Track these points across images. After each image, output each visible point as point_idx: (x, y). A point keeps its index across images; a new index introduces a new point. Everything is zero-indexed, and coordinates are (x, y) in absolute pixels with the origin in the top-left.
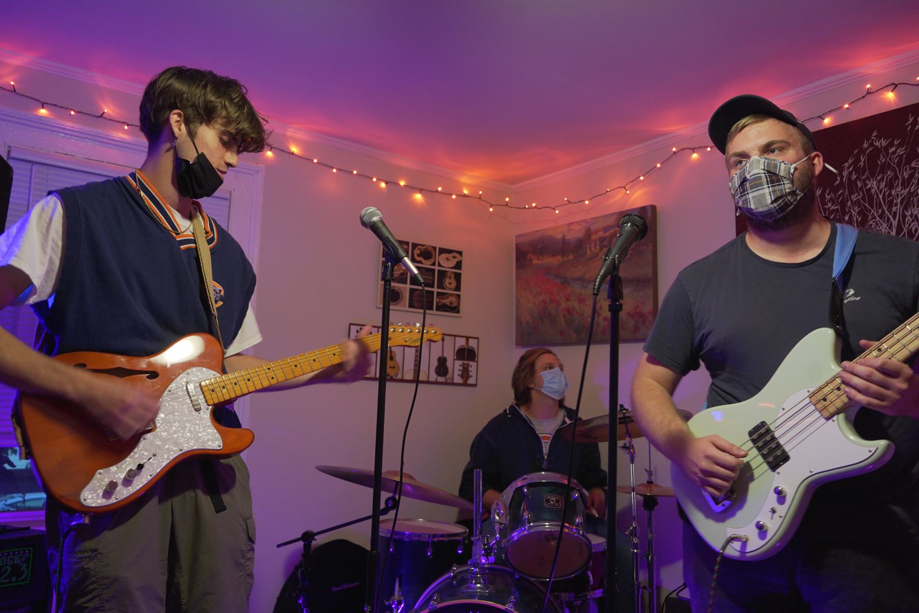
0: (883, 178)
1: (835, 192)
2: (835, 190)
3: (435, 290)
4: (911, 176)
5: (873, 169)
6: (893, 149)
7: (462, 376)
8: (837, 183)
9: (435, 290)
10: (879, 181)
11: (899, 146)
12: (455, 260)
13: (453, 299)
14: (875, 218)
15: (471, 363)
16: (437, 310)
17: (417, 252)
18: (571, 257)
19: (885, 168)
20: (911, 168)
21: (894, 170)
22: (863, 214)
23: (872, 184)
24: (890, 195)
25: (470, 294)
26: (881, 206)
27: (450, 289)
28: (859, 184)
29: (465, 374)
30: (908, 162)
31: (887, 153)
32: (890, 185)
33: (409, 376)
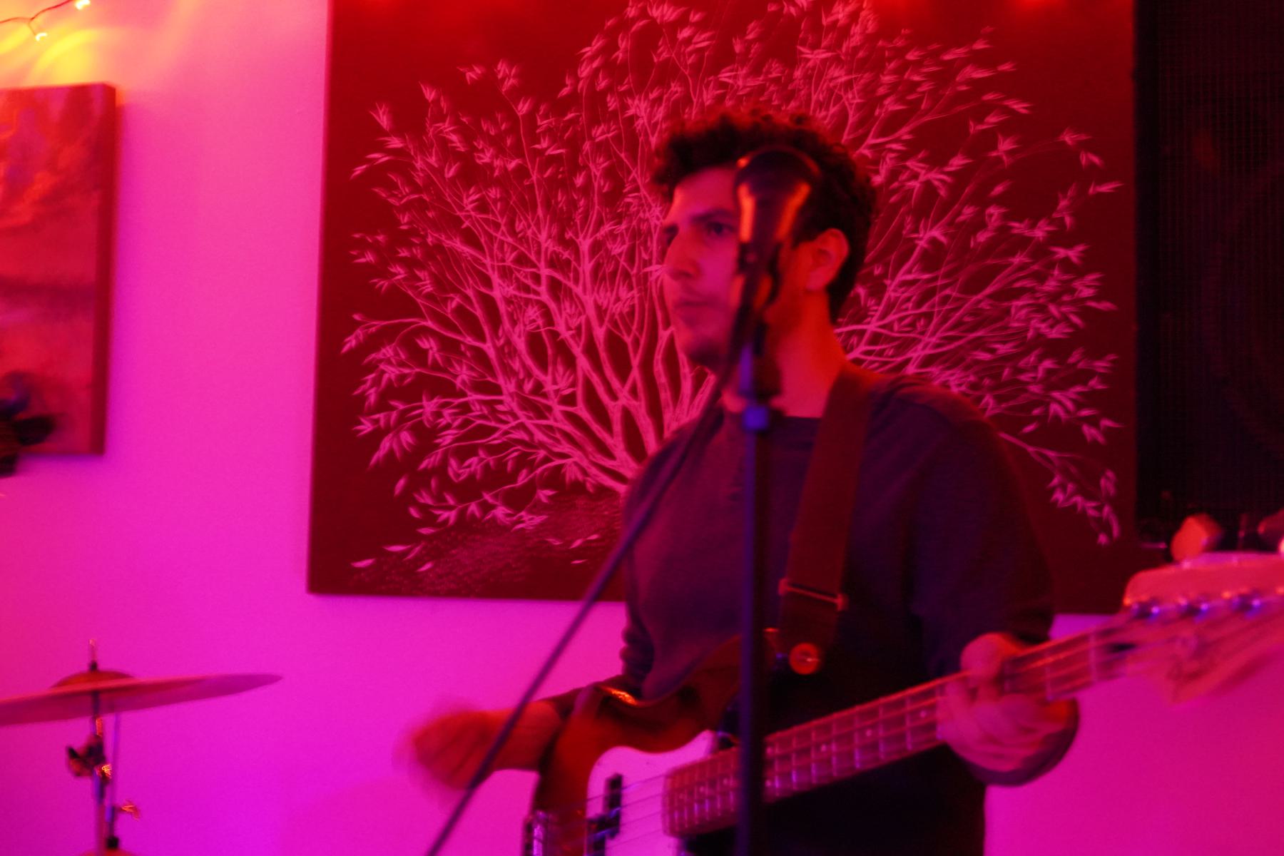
0: (658, 101)
2: (560, 108)
8: (565, 91)
11: (700, 27)
14: (637, 189)
19: (668, 73)
20: (723, 85)
22: (615, 174)
23: (638, 107)
28: (612, 103)
30: (716, 71)
31: (673, 39)
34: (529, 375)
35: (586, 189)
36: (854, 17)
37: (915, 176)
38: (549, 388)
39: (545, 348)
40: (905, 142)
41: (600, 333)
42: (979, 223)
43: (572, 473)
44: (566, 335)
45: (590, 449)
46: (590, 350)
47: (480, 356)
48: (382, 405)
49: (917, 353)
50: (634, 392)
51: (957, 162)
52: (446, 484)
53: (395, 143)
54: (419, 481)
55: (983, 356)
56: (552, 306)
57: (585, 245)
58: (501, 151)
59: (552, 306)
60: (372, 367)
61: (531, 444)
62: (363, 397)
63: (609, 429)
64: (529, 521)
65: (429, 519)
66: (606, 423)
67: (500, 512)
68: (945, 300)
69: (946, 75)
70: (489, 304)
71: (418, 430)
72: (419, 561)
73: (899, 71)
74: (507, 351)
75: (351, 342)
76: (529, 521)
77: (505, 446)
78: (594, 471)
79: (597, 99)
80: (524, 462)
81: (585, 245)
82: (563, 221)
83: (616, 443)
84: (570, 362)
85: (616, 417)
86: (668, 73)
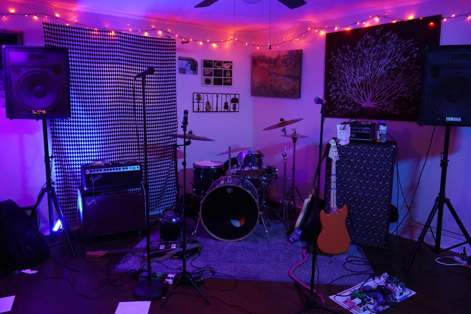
2: (355, 51)
3: (223, 77)
4: (376, 49)
5: (366, 46)
7: (233, 109)
9: (223, 77)
11: (373, 39)
13: (229, 80)
18: (272, 65)
19: (369, 46)
23: (365, 51)
29: (234, 108)
32: (370, 52)
33: (215, 110)
36: (394, 37)
39: (353, 85)
41: (360, 83)
43: (356, 102)
46: (358, 85)
47: (345, 86)
48: (333, 93)
49: (401, 85)
51: (408, 57)
52: (340, 103)
53: (334, 57)
54: (337, 103)
57: (358, 71)
58: (347, 58)
60: (331, 87)
61: (351, 98)
63: (360, 96)
64: (351, 108)
65: (338, 108)
69: (407, 45)
70: (346, 79)
71: (337, 96)
72: (337, 113)
73: (401, 44)
74: (348, 85)
75: (329, 84)
76: (351, 108)
79: (360, 50)
80: (350, 100)
81: (358, 71)
82: (355, 67)
83: (361, 98)
84: (356, 87)
85: (362, 94)
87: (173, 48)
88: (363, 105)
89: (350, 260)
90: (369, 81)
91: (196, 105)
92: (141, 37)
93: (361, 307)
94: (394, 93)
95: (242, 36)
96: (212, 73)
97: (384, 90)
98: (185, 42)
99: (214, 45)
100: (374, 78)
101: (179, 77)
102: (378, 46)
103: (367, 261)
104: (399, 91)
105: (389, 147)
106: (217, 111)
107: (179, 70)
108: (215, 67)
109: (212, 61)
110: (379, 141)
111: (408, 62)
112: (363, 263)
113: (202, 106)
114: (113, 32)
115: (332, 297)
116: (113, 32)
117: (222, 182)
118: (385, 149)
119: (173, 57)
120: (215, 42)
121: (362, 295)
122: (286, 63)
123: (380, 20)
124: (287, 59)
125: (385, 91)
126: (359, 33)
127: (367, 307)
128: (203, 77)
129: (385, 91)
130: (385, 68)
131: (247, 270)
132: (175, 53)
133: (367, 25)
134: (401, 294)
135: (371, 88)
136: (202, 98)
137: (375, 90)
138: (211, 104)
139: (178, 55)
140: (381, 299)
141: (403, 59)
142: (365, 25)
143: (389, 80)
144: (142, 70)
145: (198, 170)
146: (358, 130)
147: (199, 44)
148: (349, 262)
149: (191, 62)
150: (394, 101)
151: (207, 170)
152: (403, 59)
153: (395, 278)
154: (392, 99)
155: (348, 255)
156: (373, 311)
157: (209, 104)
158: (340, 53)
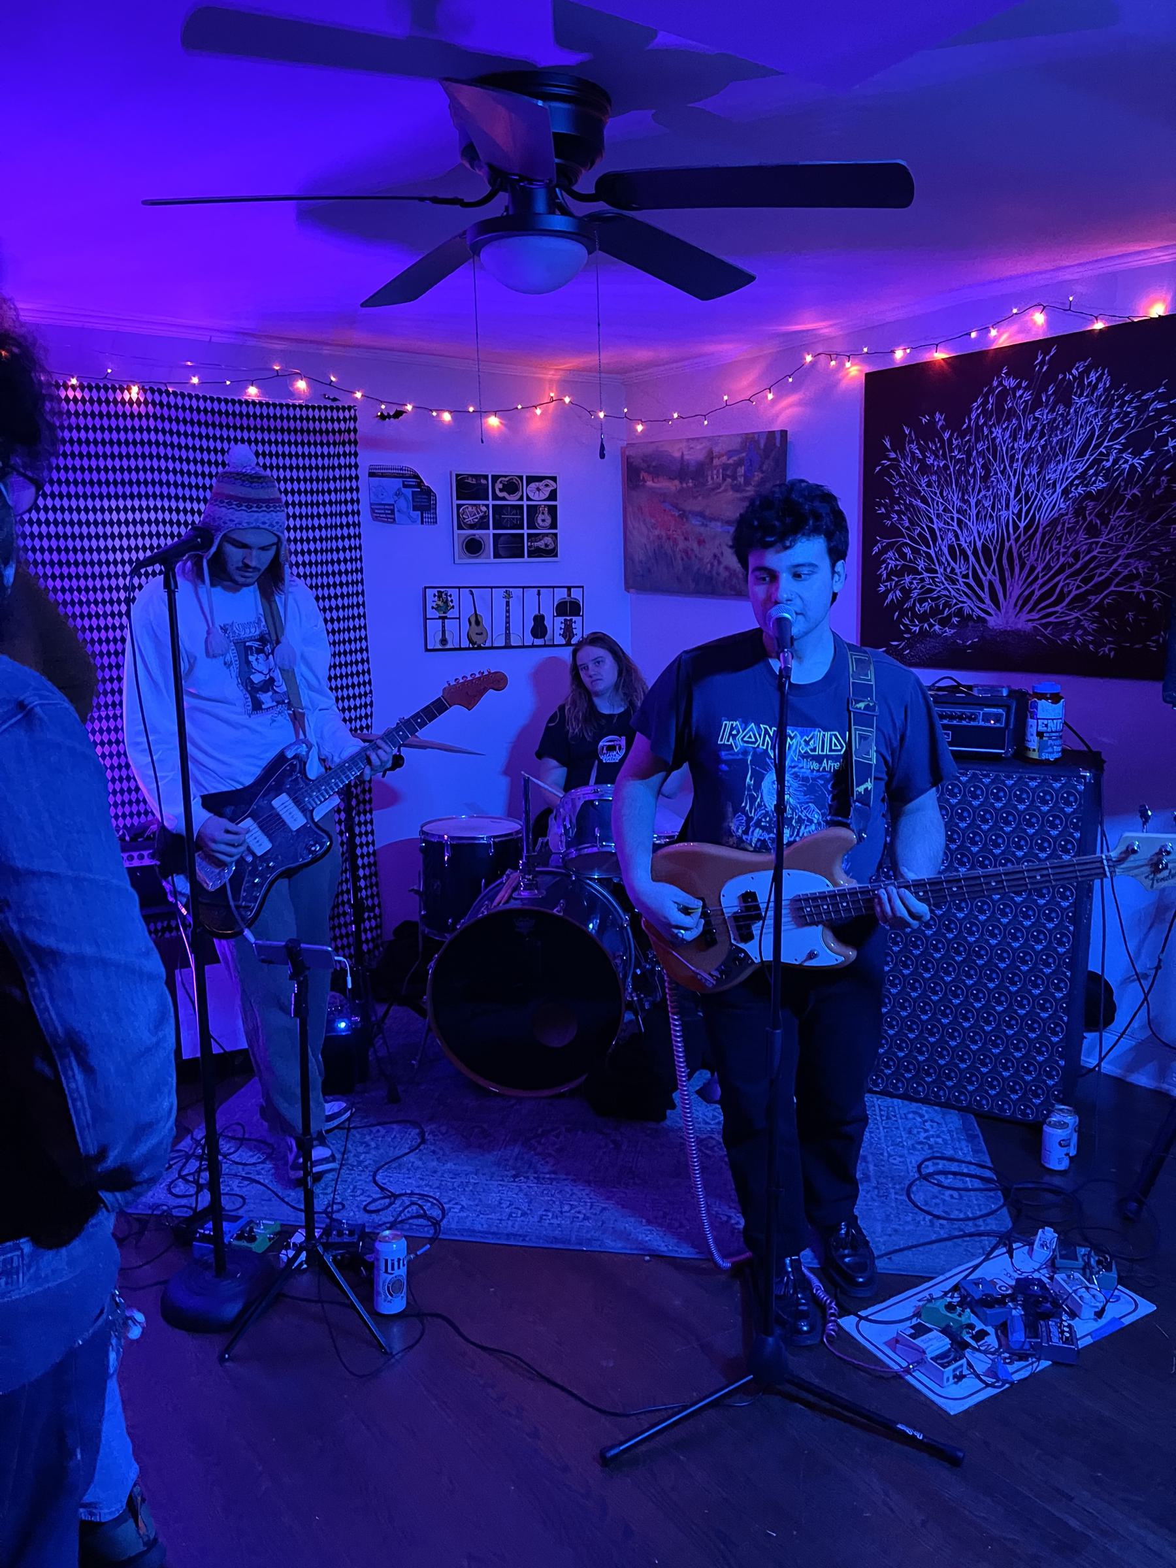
1: (963, 438)
2: (962, 435)
3: (525, 531)
5: (1001, 413)
6: (1021, 392)
7: (564, 636)
10: (1004, 430)
11: (1026, 389)
12: (550, 489)
14: (996, 473)
15: (574, 619)
16: (529, 556)
17: (499, 486)
19: (1012, 413)
20: (1035, 418)
21: (1019, 419)
24: (1013, 448)
25: (570, 530)
26: (1003, 461)
27: (543, 528)
29: (568, 632)
30: (1033, 411)
32: (1014, 437)
34: (949, 564)
35: (974, 475)
36: (1099, 379)
37: (1126, 461)
38: (958, 571)
40: (1122, 444)
41: (979, 544)
42: (1156, 485)
43: (967, 611)
44: (965, 545)
45: (974, 599)
46: (975, 553)
47: (928, 555)
48: (889, 579)
49: (1125, 552)
50: (994, 572)
51: (1147, 453)
52: (915, 614)
53: (893, 455)
54: (904, 614)
55: (1157, 553)
56: (959, 532)
57: (973, 502)
58: (937, 457)
59: (959, 532)
60: (884, 561)
62: (881, 575)
64: (949, 632)
65: (908, 630)
66: (982, 587)
67: (937, 627)
68: (1138, 525)
70: (932, 531)
71: (903, 590)
72: (904, 649)
74: (939, 553)
75: (876, 550)
76: (949, 632)
77: (939, 597)
78: (976, 609)
79: (979, 429)
80: (947, 605)
81: (973, 502)
82: (964, 490)
83: (986, 596)
84: (966, 559)
85: (986, 584)
86: (1012, 413)
87: (351, 439)
88: (992, 622)
89: (931, 1170)
90: (1013, 537)
91: (434, 626)
92: (233, 402)
93: (944, 1367)
94: (1097, 579)
95: (590, 388)
96: (486, 516)
97: (1061, 570)
98: (389, 416)
99: (493, 421)
100: (1027, 528)
101: (372, 534)
102: (1043, 414)
103: (988, 1174)
104: (1116, 573)
105: (1069, 778)
106: (508, 646)
107: (373, 511)
108: (495, 497)
109: (486, 477)
110: (1035, 755)
111: (1145, 468)
112: (978, 1184)
113: (457, 633)
114: (135, 389)
115: (848, 1323)
116: (135, 389)
117: (503, 895)
118: (1057, 785)
119: (350, 466)
120: (495, 413)
121: (954, 1316)
122: (734, 477)
123: (1048, 322)
124: (739, 463)
125: (1068, 572)
126: (975, 368)
127: (970, 1365)
128: (457, 531)
129: (1068, 572)
130: (1066, 492)
131: (566, 1208)
132: (356, 455)
133: (1001, 338)
134: (1099, 1314)
135: (1017, 562)
136: (455, 603)
137: (1033, 569)
138: (486, 623)
139: (367, 459)
140: (1018, 1336)
141: (1130, 460)
142: (996, 338)
143: (1082, 536)
144: (172, 535)
145: (432, 847)
146: (961, 718)
147: (439, 419)
148: (926, 1178)
149: (412, 482)
150: (1099, 607)
151: (465, 848)
152: (1130, 460)
153: (1082, 1251)
154: (1089, 602)
155: (928, 1153)
156: (990, 1380)
157: (478, 623)
158: (911, 442)
